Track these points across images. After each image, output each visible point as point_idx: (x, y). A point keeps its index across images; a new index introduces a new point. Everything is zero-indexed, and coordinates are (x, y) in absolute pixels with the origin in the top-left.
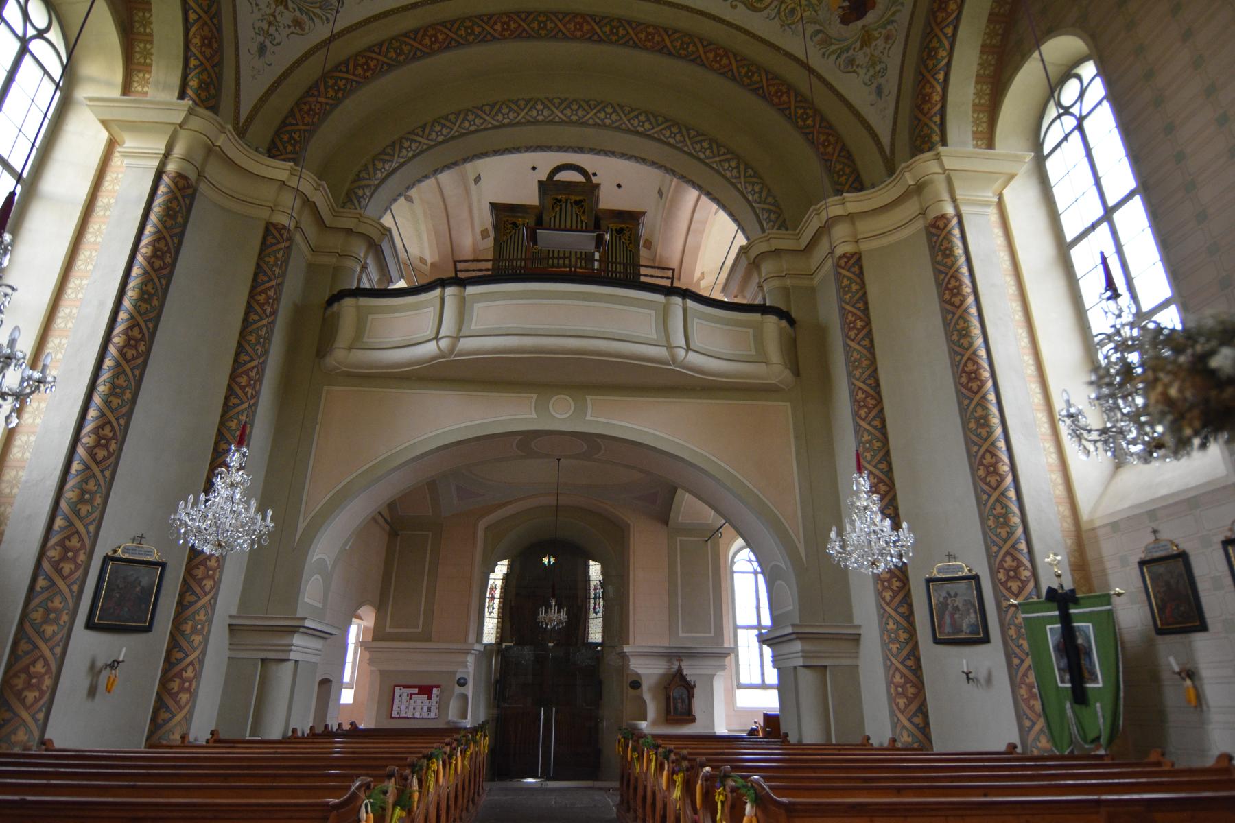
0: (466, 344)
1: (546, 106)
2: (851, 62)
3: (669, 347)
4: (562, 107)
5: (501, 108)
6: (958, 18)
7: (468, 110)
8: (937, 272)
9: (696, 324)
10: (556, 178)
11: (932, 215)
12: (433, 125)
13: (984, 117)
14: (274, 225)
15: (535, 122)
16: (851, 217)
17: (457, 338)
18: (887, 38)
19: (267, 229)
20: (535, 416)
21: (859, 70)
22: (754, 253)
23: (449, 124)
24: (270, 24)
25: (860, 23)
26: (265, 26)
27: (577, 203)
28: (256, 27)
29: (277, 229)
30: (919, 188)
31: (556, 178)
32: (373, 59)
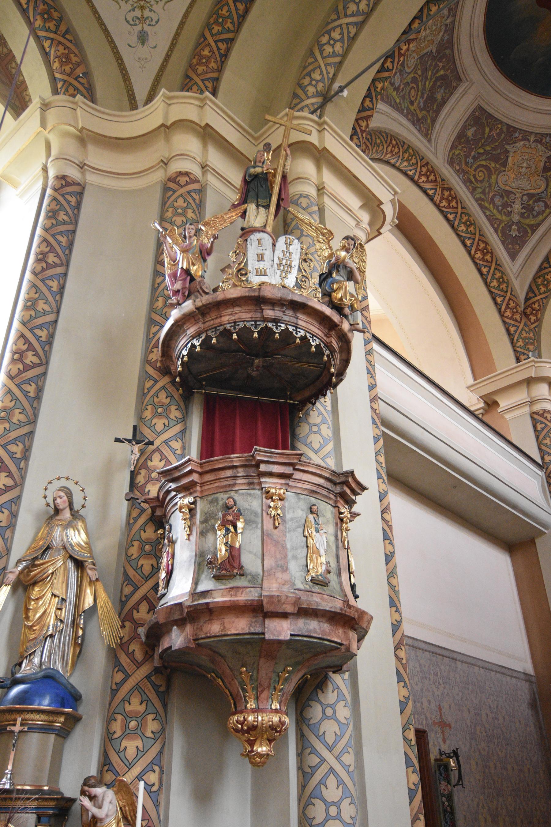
26: (138, 13)
28: (130, 19)
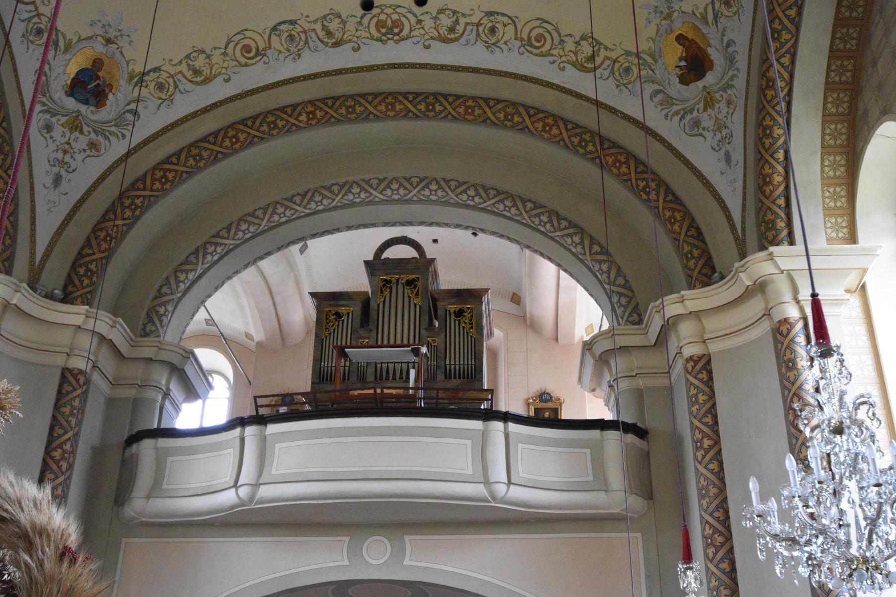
0: (266, 491)
1: (363, 189)
2: (697, 123)
3: (487, 482)
4: (382, 187)
5: (313, 195)
6: (790, 93)
7: (278, 203)
8: (783, 387)
9: (520, 451)
10: (384, 256)
11: (777, 318)
12: (239, 225)
13: (842, 191)
14: (70, 370)
15: (353, 205)
16: (697, 315)
17: (256, 485)
18: (729, 103)
19: (63, 376)
20: (347, 563)
21: (705, 133)
22: (599, 349)
23: (256, 221)
24: (65, 152)
25: (700, 84)
26: (60, 155)
27: (409, 283)
28: (51, 159)
29: (72, 375)
30: (760, 287)
31: (384, 256)
32: (170, 170)
